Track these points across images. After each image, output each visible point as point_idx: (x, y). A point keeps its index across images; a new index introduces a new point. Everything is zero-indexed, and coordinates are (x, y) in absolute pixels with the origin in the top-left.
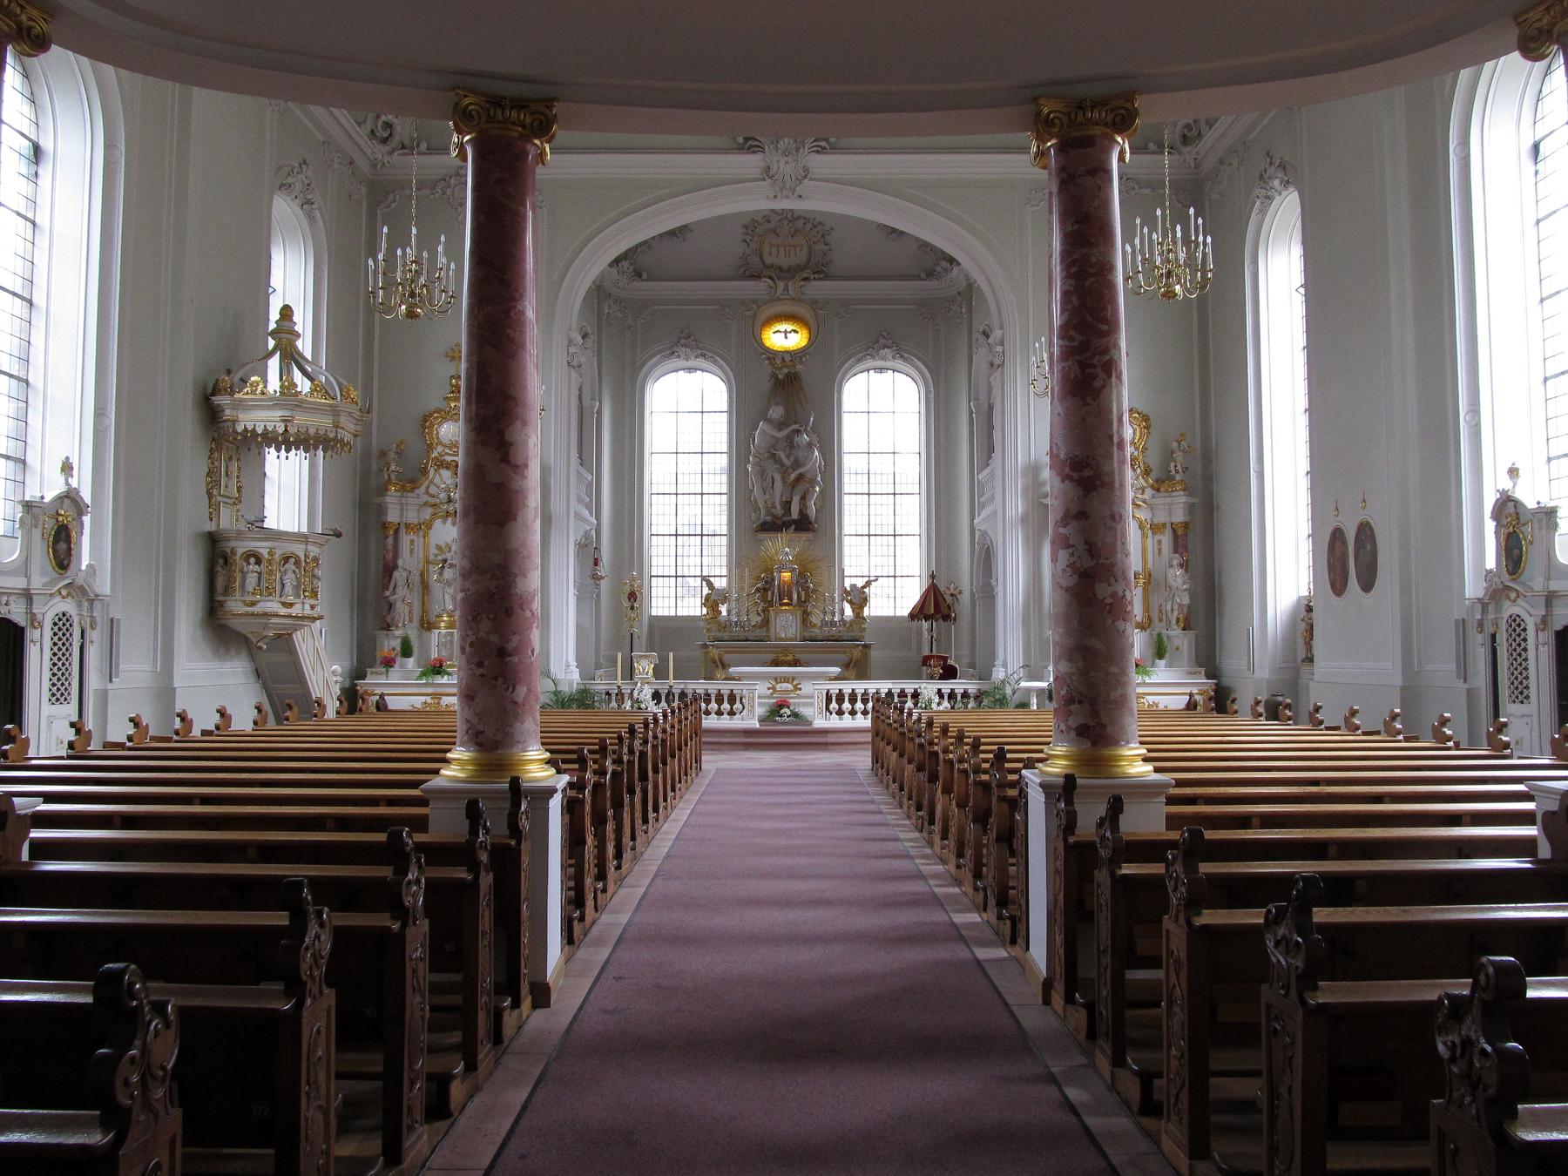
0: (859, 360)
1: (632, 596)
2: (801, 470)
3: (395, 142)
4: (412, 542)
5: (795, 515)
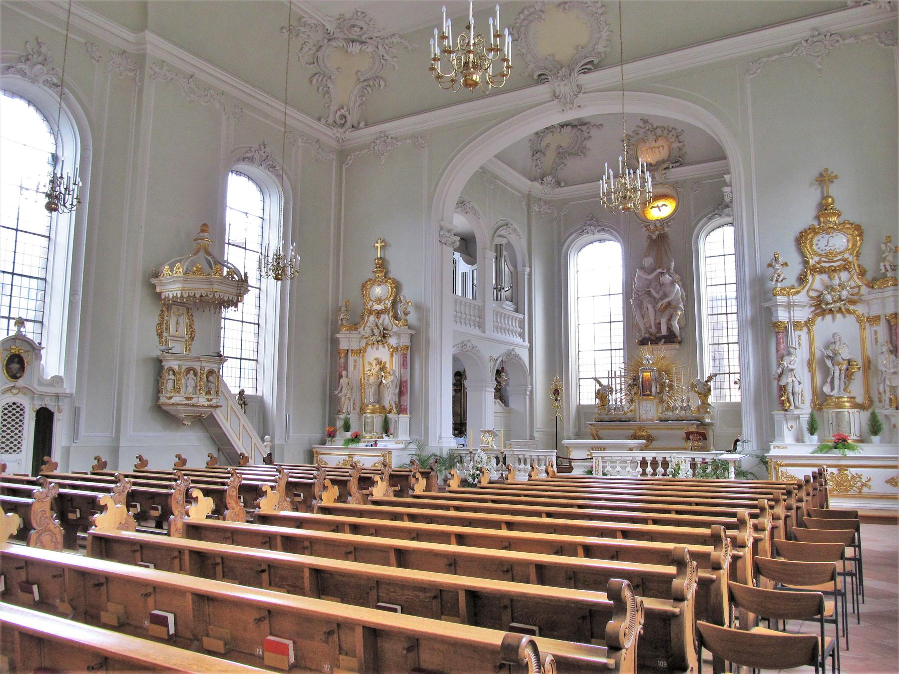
0: (710, 219)
1: (556, 392)
2: (667, 300)
3: (349, 124)
4: (355, 361)
5: (664, 331)
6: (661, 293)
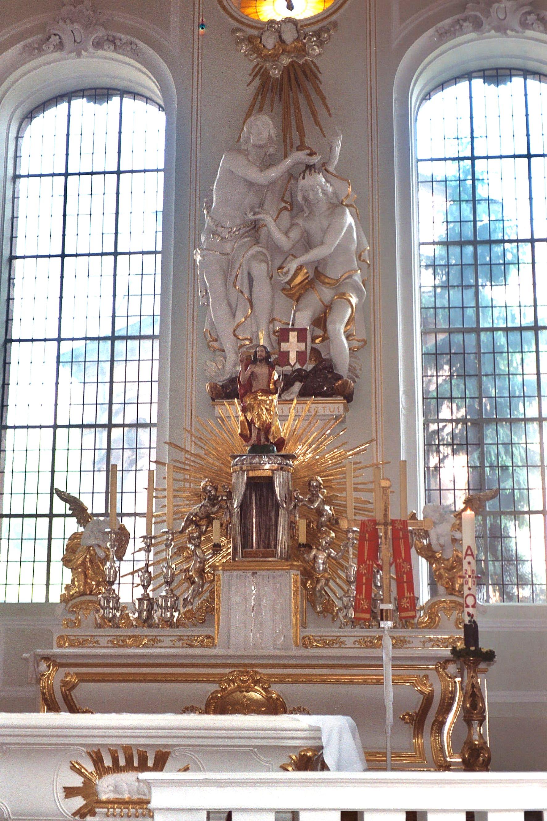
0: (444, 35)
6: (295, 234)
